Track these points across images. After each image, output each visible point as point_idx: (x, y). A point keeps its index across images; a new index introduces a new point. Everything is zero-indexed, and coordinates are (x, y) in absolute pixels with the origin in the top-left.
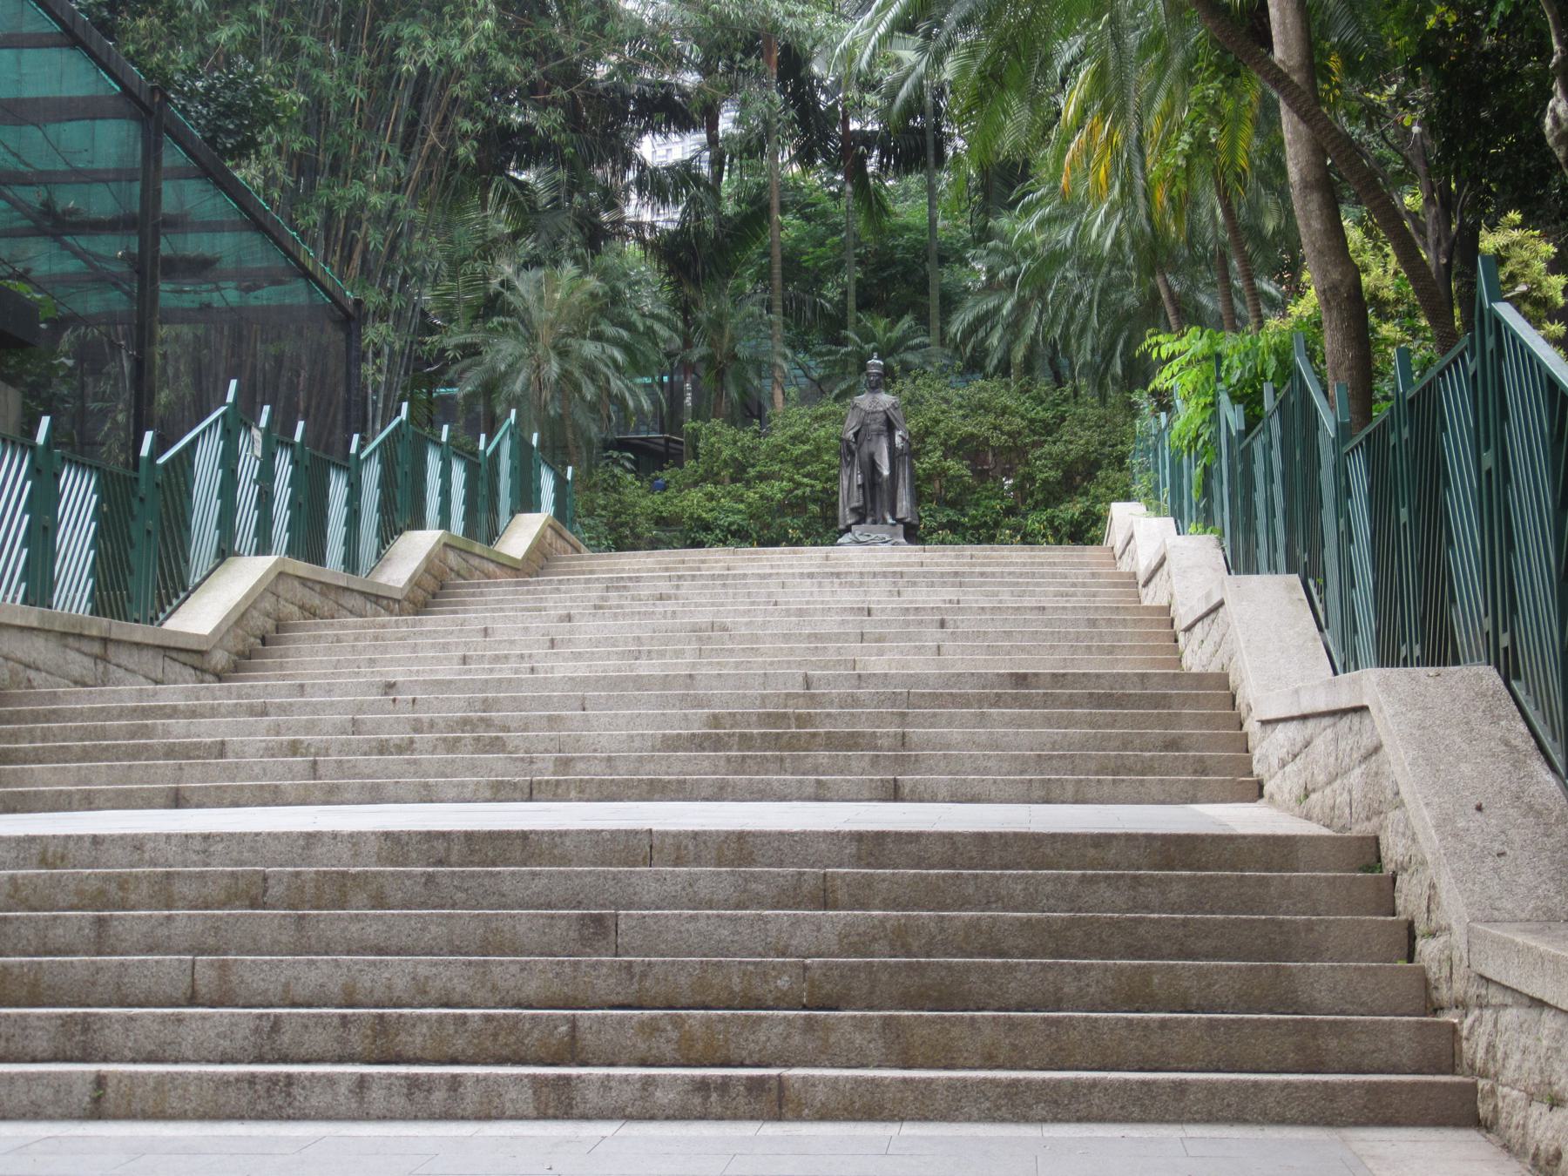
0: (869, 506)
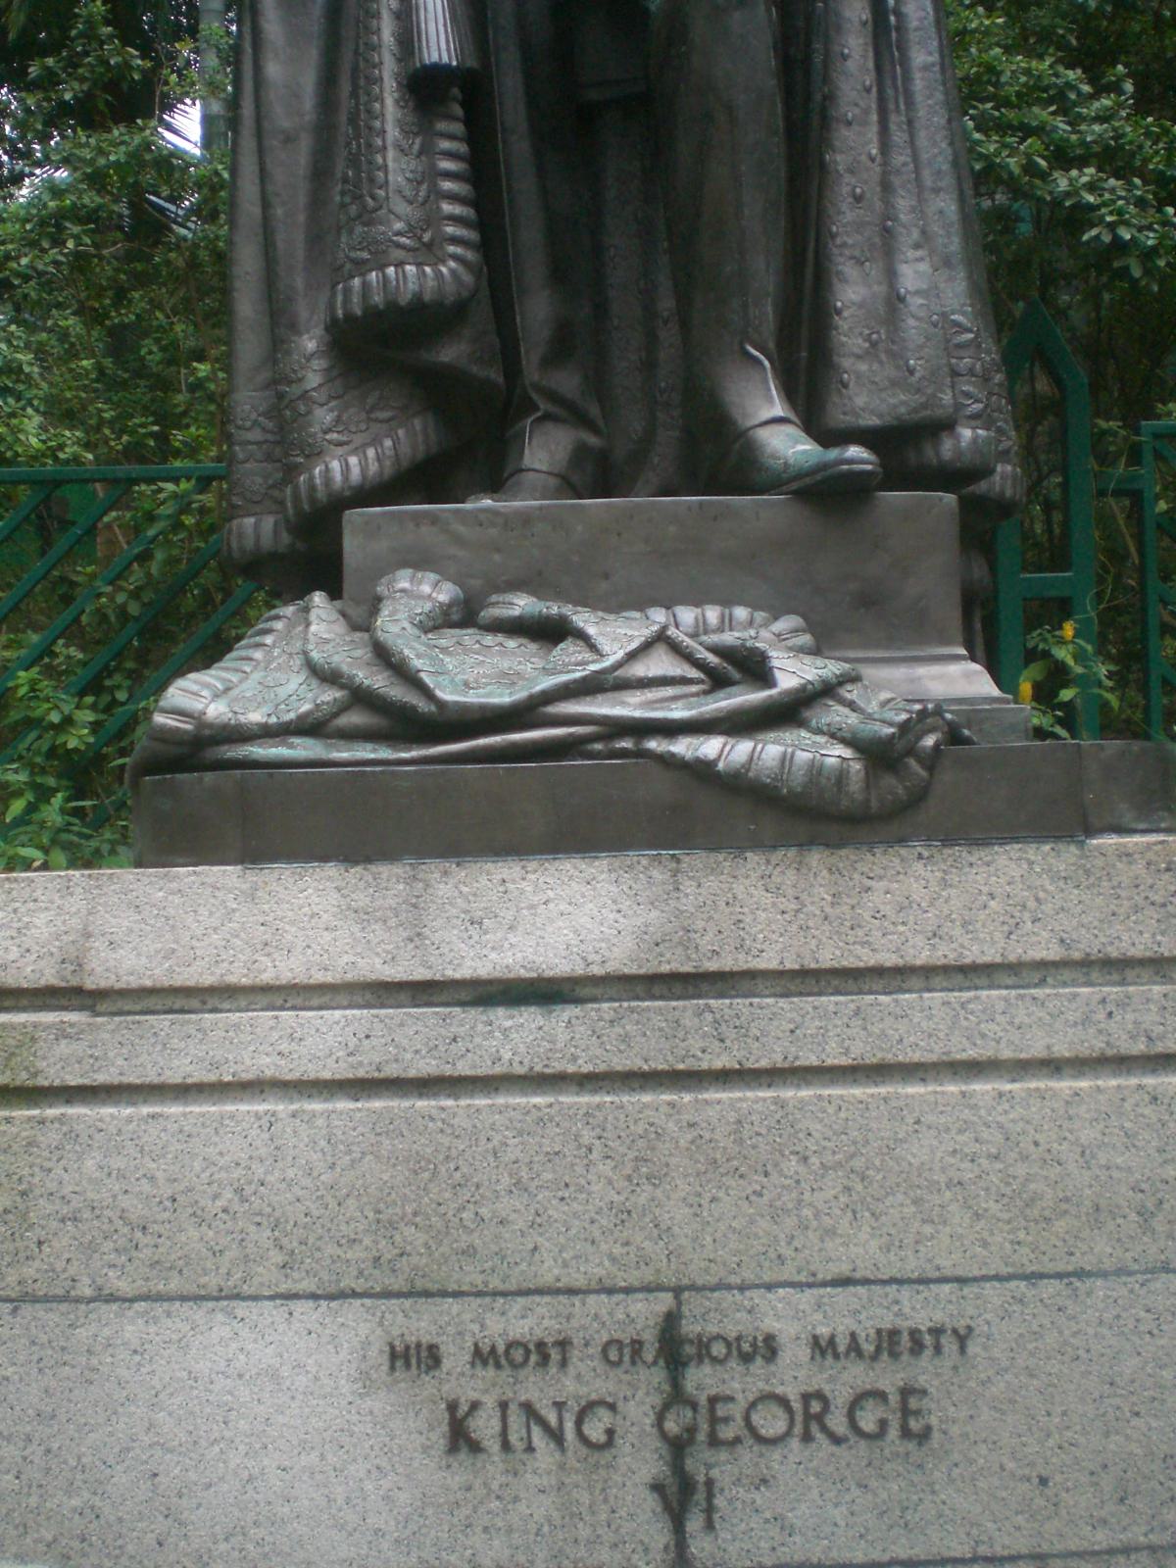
0: (537, 311)
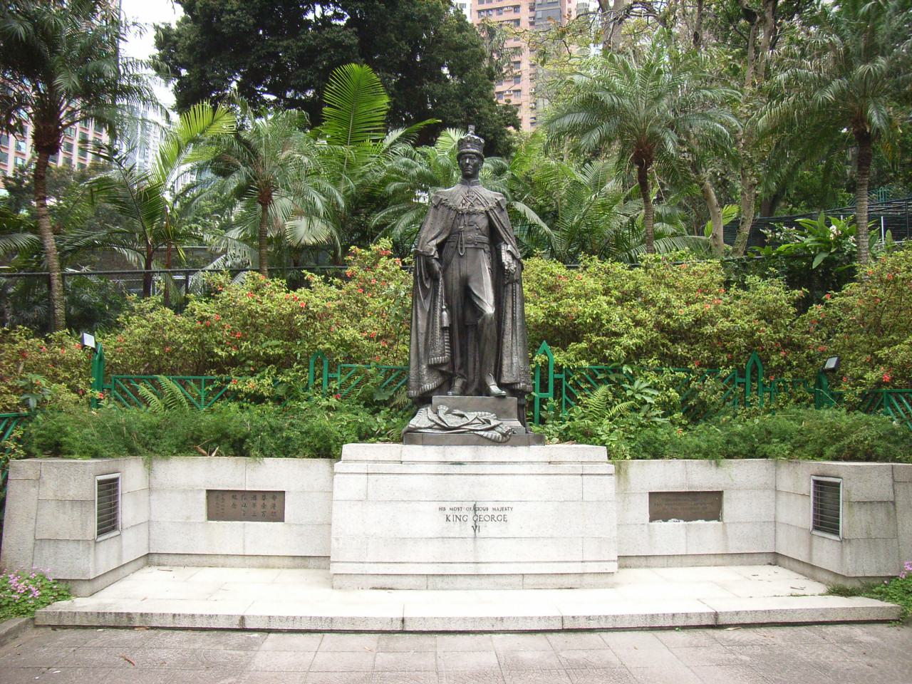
0: (458, 361)
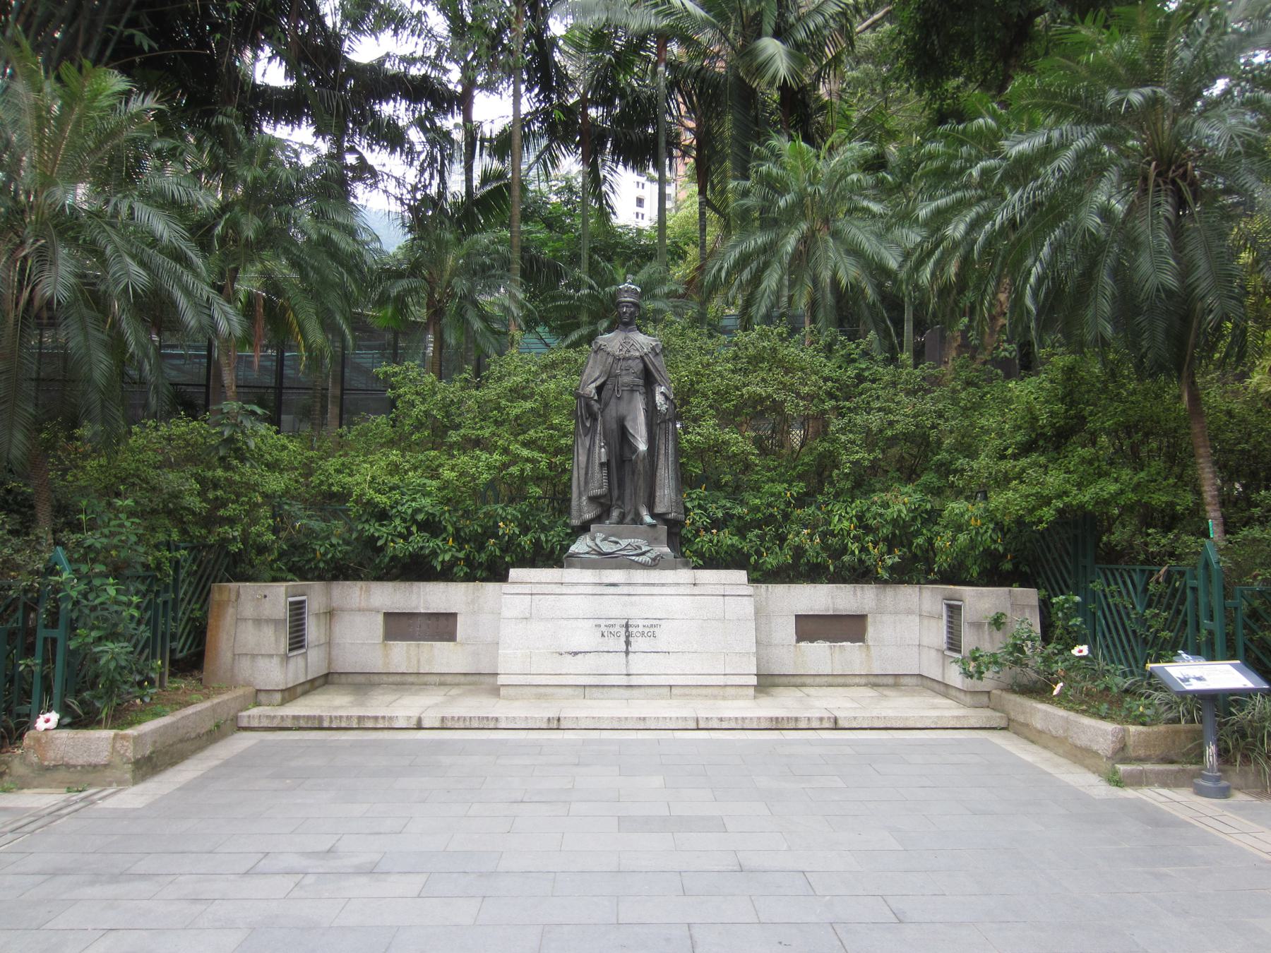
0: (615, 493)
